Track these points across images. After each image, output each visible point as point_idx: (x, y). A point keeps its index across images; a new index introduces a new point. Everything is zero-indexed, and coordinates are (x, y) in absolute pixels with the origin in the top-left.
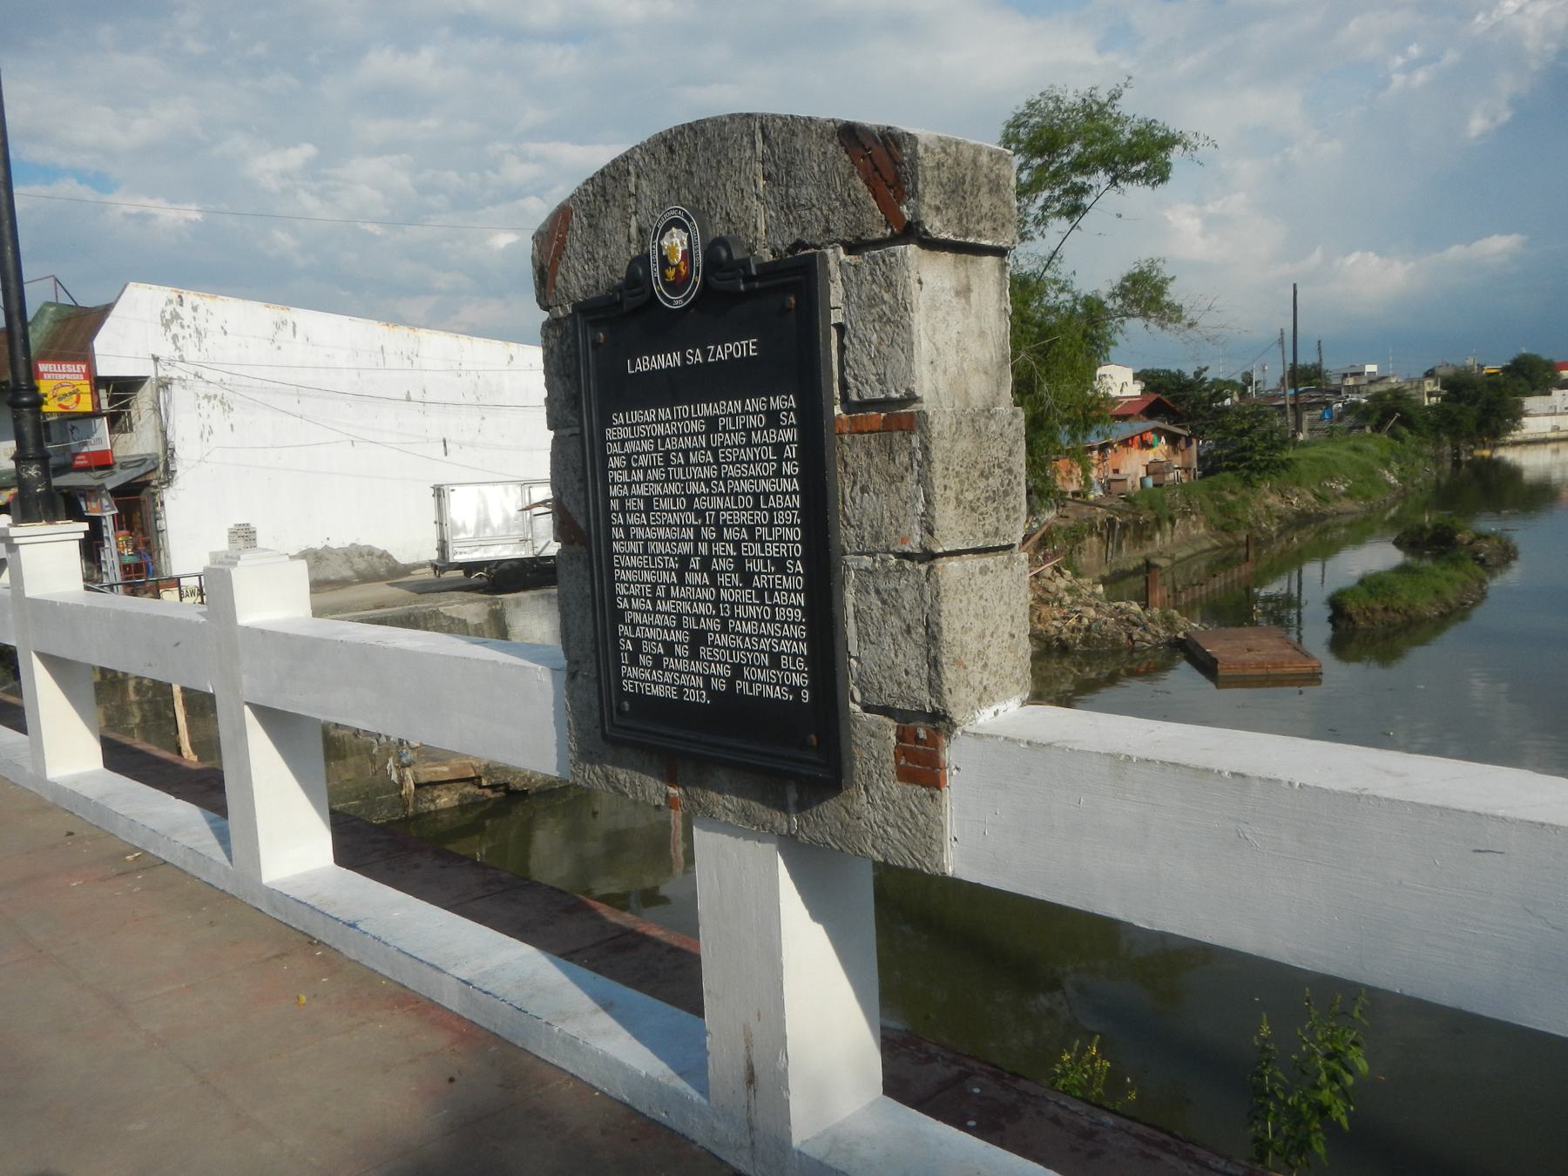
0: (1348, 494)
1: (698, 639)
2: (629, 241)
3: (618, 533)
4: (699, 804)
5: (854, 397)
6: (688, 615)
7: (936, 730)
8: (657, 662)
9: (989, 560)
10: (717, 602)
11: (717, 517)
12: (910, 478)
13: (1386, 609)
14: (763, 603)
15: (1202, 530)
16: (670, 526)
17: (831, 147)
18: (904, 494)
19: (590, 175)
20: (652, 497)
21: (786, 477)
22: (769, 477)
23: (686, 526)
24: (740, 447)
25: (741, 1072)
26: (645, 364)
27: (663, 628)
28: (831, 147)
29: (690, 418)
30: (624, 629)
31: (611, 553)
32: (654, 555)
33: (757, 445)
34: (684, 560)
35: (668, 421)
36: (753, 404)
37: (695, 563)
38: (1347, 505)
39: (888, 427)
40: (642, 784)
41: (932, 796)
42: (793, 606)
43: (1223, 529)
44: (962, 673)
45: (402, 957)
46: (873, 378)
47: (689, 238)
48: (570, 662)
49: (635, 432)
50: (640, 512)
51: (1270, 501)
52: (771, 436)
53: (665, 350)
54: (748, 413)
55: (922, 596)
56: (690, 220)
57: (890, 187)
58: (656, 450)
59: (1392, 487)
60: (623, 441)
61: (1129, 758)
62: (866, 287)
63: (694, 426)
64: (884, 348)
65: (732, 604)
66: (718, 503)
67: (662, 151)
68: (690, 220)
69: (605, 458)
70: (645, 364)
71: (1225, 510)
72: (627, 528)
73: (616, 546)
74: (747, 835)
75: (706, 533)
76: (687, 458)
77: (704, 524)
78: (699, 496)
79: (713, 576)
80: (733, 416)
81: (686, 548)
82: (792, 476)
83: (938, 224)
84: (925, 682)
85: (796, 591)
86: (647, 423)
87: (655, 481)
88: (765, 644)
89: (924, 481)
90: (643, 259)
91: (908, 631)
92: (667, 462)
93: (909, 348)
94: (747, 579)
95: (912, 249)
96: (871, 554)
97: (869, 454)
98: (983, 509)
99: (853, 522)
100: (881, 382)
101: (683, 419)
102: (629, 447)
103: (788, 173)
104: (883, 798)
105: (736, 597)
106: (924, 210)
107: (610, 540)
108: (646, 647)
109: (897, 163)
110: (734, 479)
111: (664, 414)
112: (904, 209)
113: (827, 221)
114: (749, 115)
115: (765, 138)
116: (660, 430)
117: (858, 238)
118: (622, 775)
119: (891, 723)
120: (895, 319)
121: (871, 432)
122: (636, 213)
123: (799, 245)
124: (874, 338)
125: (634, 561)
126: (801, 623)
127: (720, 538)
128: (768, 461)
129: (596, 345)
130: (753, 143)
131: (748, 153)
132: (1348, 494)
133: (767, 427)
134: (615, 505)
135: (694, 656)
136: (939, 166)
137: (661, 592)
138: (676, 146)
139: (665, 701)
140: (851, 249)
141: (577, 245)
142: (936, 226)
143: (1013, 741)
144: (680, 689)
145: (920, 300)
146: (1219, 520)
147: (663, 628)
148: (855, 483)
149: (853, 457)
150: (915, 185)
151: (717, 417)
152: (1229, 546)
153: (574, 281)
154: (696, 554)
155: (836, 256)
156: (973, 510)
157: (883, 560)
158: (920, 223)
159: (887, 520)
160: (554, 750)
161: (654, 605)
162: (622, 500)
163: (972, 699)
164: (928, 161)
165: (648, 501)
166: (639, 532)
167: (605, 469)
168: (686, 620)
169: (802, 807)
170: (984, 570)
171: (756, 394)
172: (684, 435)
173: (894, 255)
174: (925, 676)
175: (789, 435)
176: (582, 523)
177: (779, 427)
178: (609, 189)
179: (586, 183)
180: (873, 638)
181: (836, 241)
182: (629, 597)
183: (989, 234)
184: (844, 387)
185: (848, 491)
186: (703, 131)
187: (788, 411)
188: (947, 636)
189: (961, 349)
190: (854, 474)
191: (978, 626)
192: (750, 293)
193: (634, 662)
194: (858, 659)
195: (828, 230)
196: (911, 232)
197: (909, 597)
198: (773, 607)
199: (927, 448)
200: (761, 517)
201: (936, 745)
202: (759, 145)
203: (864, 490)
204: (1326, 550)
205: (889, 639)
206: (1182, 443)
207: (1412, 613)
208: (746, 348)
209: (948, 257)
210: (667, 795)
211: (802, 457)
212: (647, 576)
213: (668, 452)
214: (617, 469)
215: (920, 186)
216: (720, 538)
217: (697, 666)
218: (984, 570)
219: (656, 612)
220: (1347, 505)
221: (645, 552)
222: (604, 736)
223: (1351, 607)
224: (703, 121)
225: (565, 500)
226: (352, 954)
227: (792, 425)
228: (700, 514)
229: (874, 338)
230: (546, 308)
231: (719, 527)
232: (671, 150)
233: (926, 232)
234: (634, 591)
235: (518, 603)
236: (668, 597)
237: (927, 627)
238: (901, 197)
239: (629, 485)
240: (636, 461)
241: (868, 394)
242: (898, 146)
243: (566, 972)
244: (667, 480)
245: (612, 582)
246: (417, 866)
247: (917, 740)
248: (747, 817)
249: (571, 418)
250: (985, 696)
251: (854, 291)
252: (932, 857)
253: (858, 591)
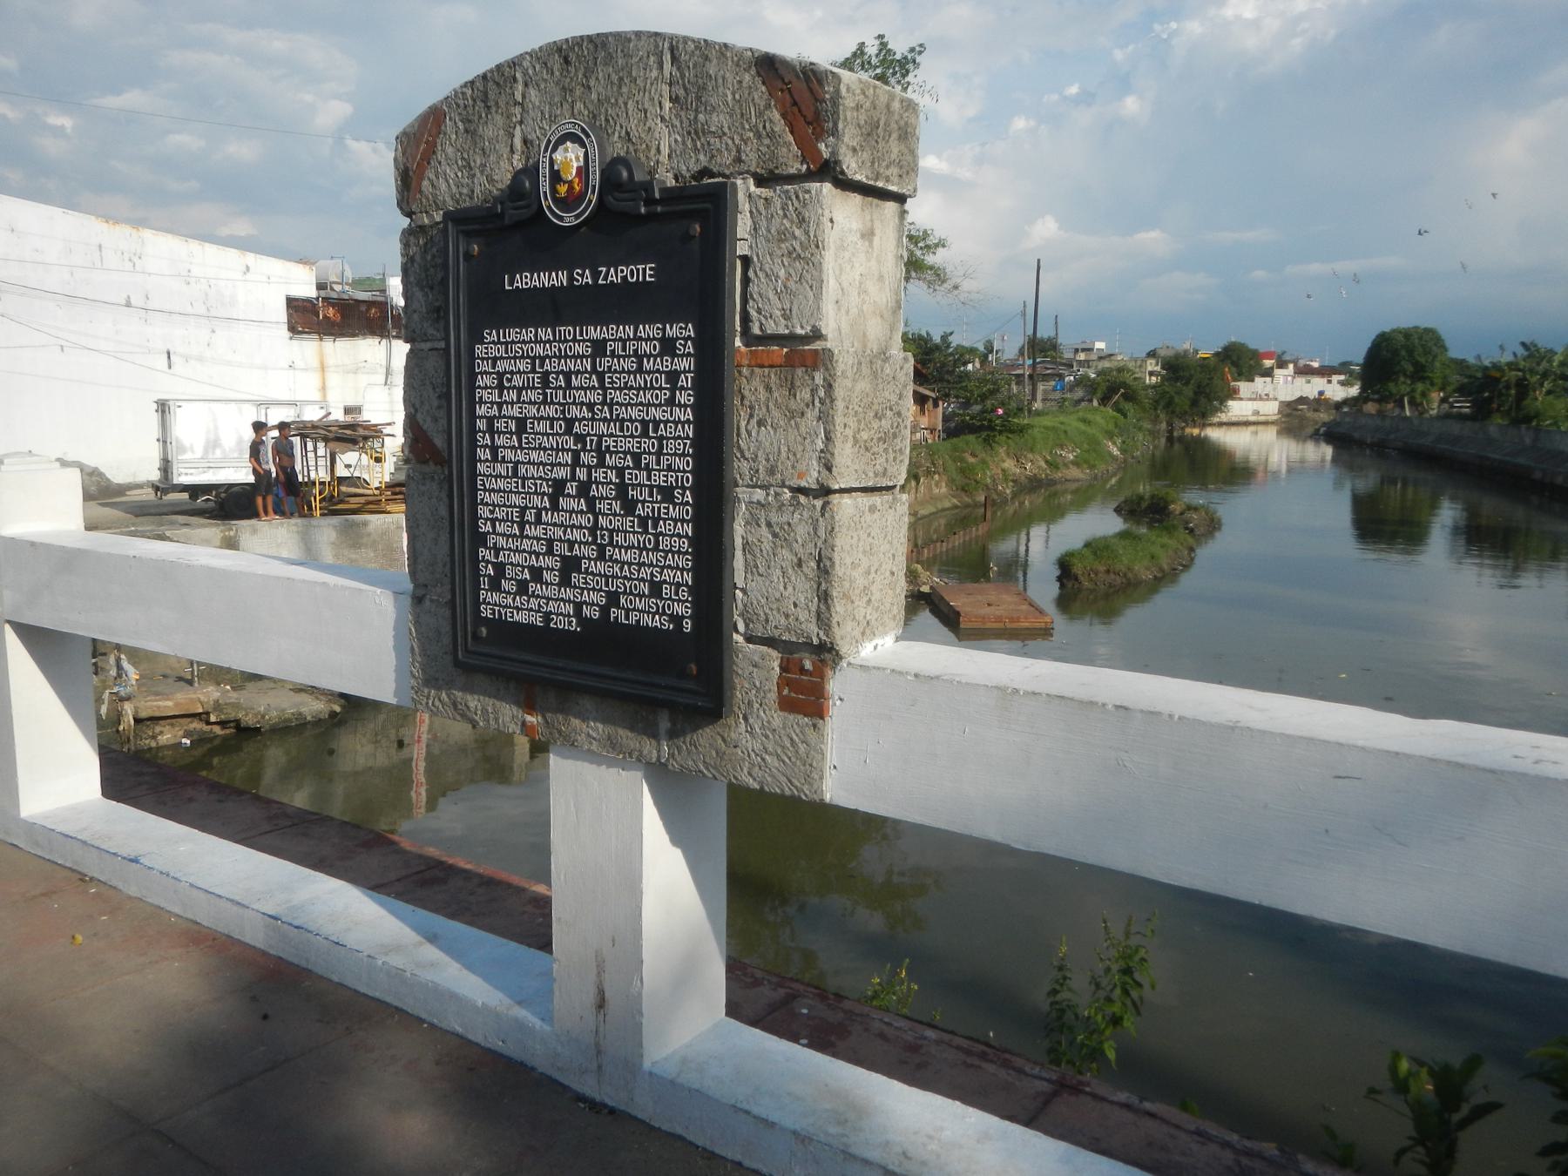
0: (1076, 463)
1: (570, 565)
2: (512, 151)
4: (560, 732)
5: (756, 330)
6: (560, 540)
7: (822, 661)
8: (522, 588)
9: (876, 499)
10: (593, 530)
11: (599, 443)
12: (811, 415)
13: (1108, 572)
14: (646, 532)
15: (944, 490)
16: (545, 449)
17: (747, 77)
18: (803, 430)
19: (470, 78)
20: (526, 418)
21: (680, 405)
22: (660, 405)
23: (563, 450)
24: (629, 372)
25: (590, 998)
26: (526, 281)
27: (530, 553)
28: (747, 77)
29: (574, 340)
30: (483, 552)
31: (474, 474)
32: (524, 479)
33: (649, 373)
34: (559, 486)
35: (549, 341)
36: (646, 330)
37: (571, 488)
38: (1074, 472)
39: (790, 362)
40: (495, 712)
41: (815, 726)
42: (679, 535)
43: (963, 489)
44: (850, 607)
45: (195, 892)
46: (778, 313)
47: (586, 154)
48: (416, 587)
49: (506, 352)
50: (511, 433)
51: (1005, 465)
52: (667, 364)
53: (549, 269)
54: (641, 339)
55: (815, 530)
56: (588, 136)
57: (809, 123)
58: (533, 371)
59: (1115, 458)
60: (495, 360)
61: (1016, 691)
62: (776, 222)
63: (579, 349)
64: (791, 284)
65: (611, 532)
66: (603, 428)
67: (556, 62)
68: (588, 136)
69: (473, 376)
70: (526, 281)
71: (965, 471)
72: (494, 449)
73: (481, 468)
74: (611, 763)
75: (585, 458)
76: (568, 381)
77: (584, 449)
78: (580, 421)
79: (591, 503)
80: (624, 341)
81: (562, 473)
82: (686, 406)
83: (854, 165)
84: (813, 614)
85: (683, 521)
86: (524, 342)
87: (530, 403)
88: (645, 573)
89: (825, 417)
90: (531, 171)
91: (800, 564)
92: (545, 383)
93: (818, 286)
94: (629, 507)
95: (827, 187)
96: (765, 487)
97: (768, 388)
98: (875, 449)
99: (747, 455)
100: (787, 317)
101: (566, 341)
103: (699, 98)
104: (763, 727)
105: (616, 523)
106: (843, 150)
107: (474, 460)
108: (509, 571)
109: (818, 99)
110: (621, 405)
111: (545, 333)
112: (822, 146)
113: (739, 151)
114: (657, 34)
115: (674, 59)
117: (771, 172)
118: (473, 702)
119: (775, 654)
120: (806, 255)
121: (771, 366)
122: (521, 122)
123: (706, 172)
124: (782, 273)
125: (501, 484)
126: (687, 553)
127: (601, 463)
128: (661, 389)
129: (468, 256)
130: (661, 67)
131: (655, 73)
132: (1076, 463)
133: (661, 355)
134: (481, 424)
135: (565, 582)
136: (858, 107)
137: (530, 516)
138: (572, 57)
139: (530, 627)
140: (761, 181)
141: (450, 150)
142: (854, 168)
143: (901, 673)
144: (547, 617)
145: (831, 237)
146: (959, 478)
147: (530, 553)
148: (751, 416)
149: (752, 390)
150: (836, 125)
151: (605, 341)
152: (967, 506)
153: (443, 186)
154: (573, 478)
155: (745, 188)
156: (867, 449)
157: (777, 494)
158: (837, 162)
159: (784, 454)
160: (392, 676)
161: (522, 529)
162: (490, 420)
163: (857, 633)
164: (848, 102)
165: (521, 423)
166: (509, 455)
167: (472, 387)
168: (557, 546)
169: (673, 735)
170: (873, 509)
171: (651, 321)
172: (566, 356)
173: (808, 192)
174: (814, 609)
176: (439, 442)
177: (673, 355)
178: (491, 95)
179: (465, 85)
180: (761, 570)
181: (747, 172)
182: (493, 521)
183: (896, 180)
184: (746, 319)
185: (743, 424)
186: (604, 45)
187: (686, 339)
188: (839, 570)
189: (862, 291)
190: (751, 407)
191: (865, 563)
192: (651, 217)
193: (495, 586)
194: (744, 591)
195: (738, 160)
196: (828, 171)
197: (802, 531)
198: (656, 536)
199: (830, 386)
200: (646, 444)
201: (822, 676)
202: (667, 66)
203: (760, 423)
204: (1053, 513)
205: (779, 572)
206: (930, 404)
207: (1130, 575)
208: (644, 272)
209: (856, 199)
210: (524, 723)
211: (698, 386)
212: (515, 499)
213: (547, 373)
214: (486, 387)
215: (840, 126)
216: (601, 463)
217: (568, 593)
218: (873, 509)
219: (522, 536)
220: (1074, 472)
221: (515, 474)
222: (457, 664)
223: (1078, 568)
224: (606, 35)
225: (419, 417)
226: (133, 891)
227: (689, 354)
228: (580, 438)
229: (782, 273)
230: (409, 214)
231: (601, 454)
232: (567, 61)
233: (842, 172)
234: (499, 514)
235: (255, 531)
236: (538, 521)
237: (819, 562)
238: (820, 134)
239: (500, 405)
240: (509, 380)
241: (771, 328)
242: (820, 82)
243: (381, 904)
244: (545, 402)
245: (474, 505)
246: (191, 800)
247: (802, 670)
248: (612, 744)
249: (431, 331)
250: (868, 631)
251: (764, 223)
252: (811, 784)
253: (747, 523)
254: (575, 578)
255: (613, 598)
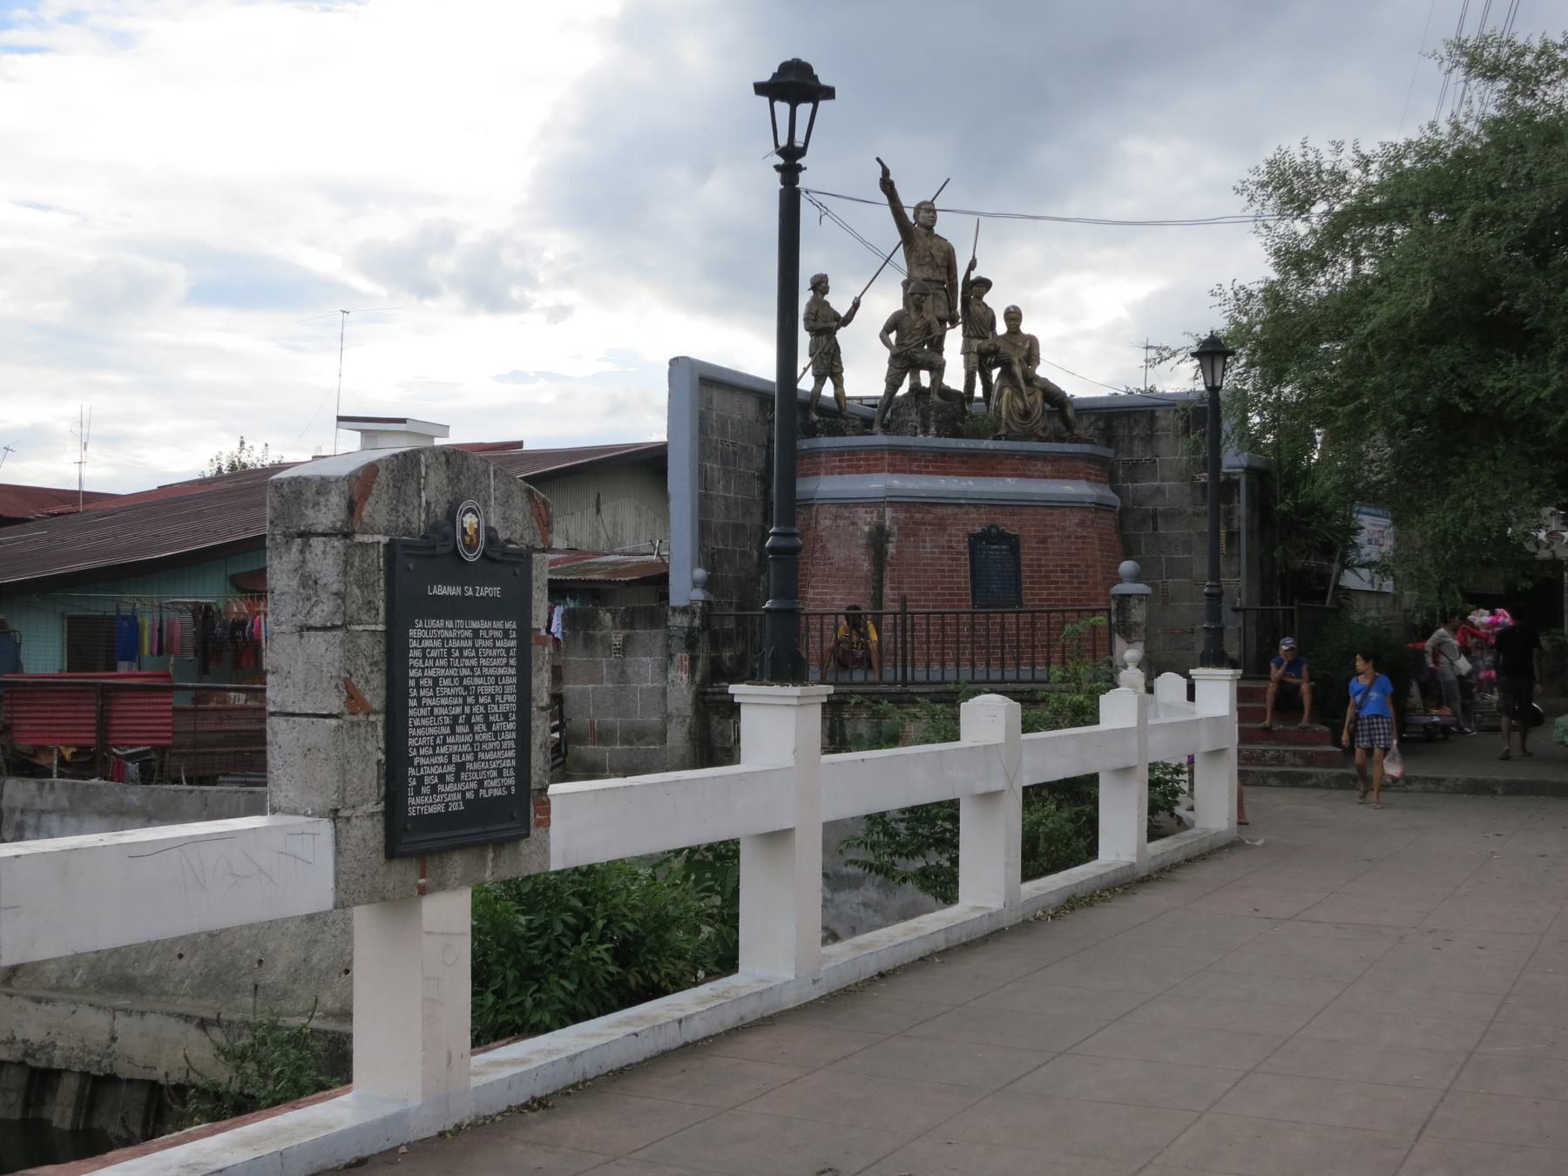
1: (461, 767)
3: (413, 703)
10: (472, 744)
26: (441, 590)
34: (455, 718)
53: (453, 584)
66: (478, 681)
70: (441, 590)
72: (419, 699)
73: (411, 712)
75: (470, 700)
79: (471, 726)
81: (458, 710)
94: (489, 725)
102: (426, 644)
107: (407, 707)
108: (427, 781)
111: (449, 624)
116: (446, 634)
127: (477, 703)
134: (412, 683)
135: (457, 780)
144: (447, 806)
162: (417, 680)
165: (436, 680)
166: (429, 702)
175: (513, 643)
193: (418, 792)
200: (498, 689)
216: (477, 703)
219: (435, 754)
228: (467, 688)
231: (477, 696)
236: (444, 743)
254: (463, 776)
255: (481, 783)
